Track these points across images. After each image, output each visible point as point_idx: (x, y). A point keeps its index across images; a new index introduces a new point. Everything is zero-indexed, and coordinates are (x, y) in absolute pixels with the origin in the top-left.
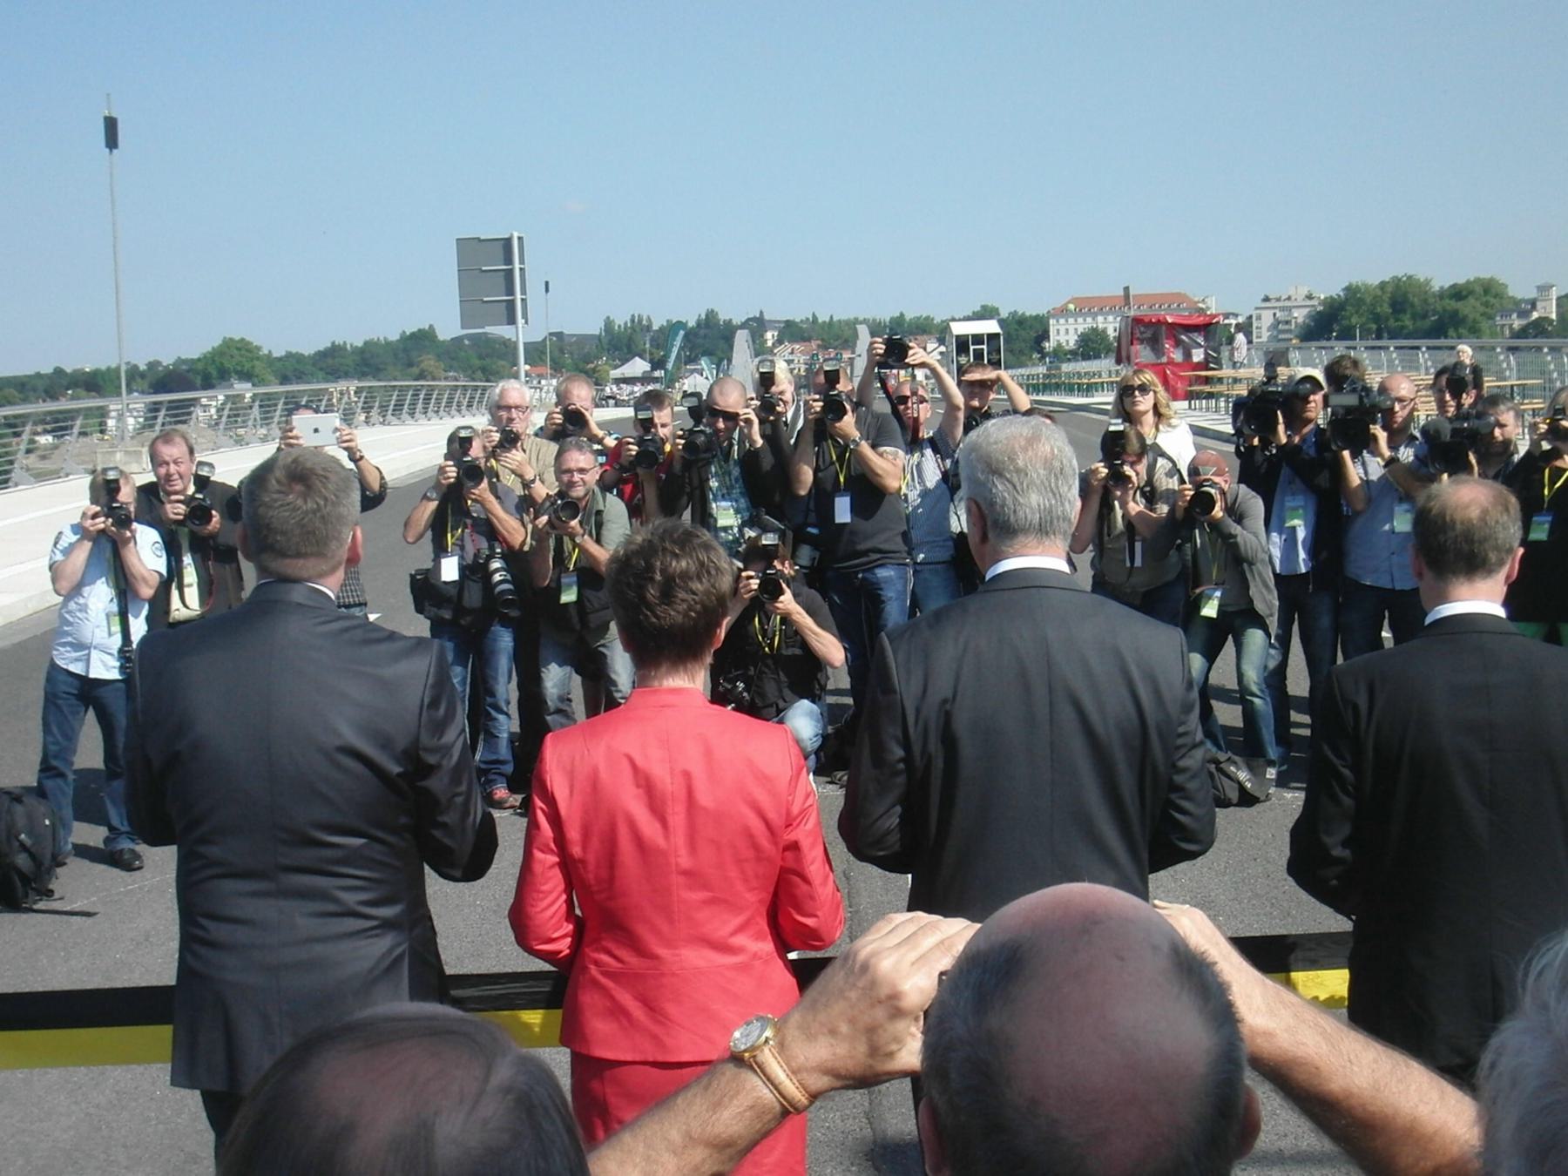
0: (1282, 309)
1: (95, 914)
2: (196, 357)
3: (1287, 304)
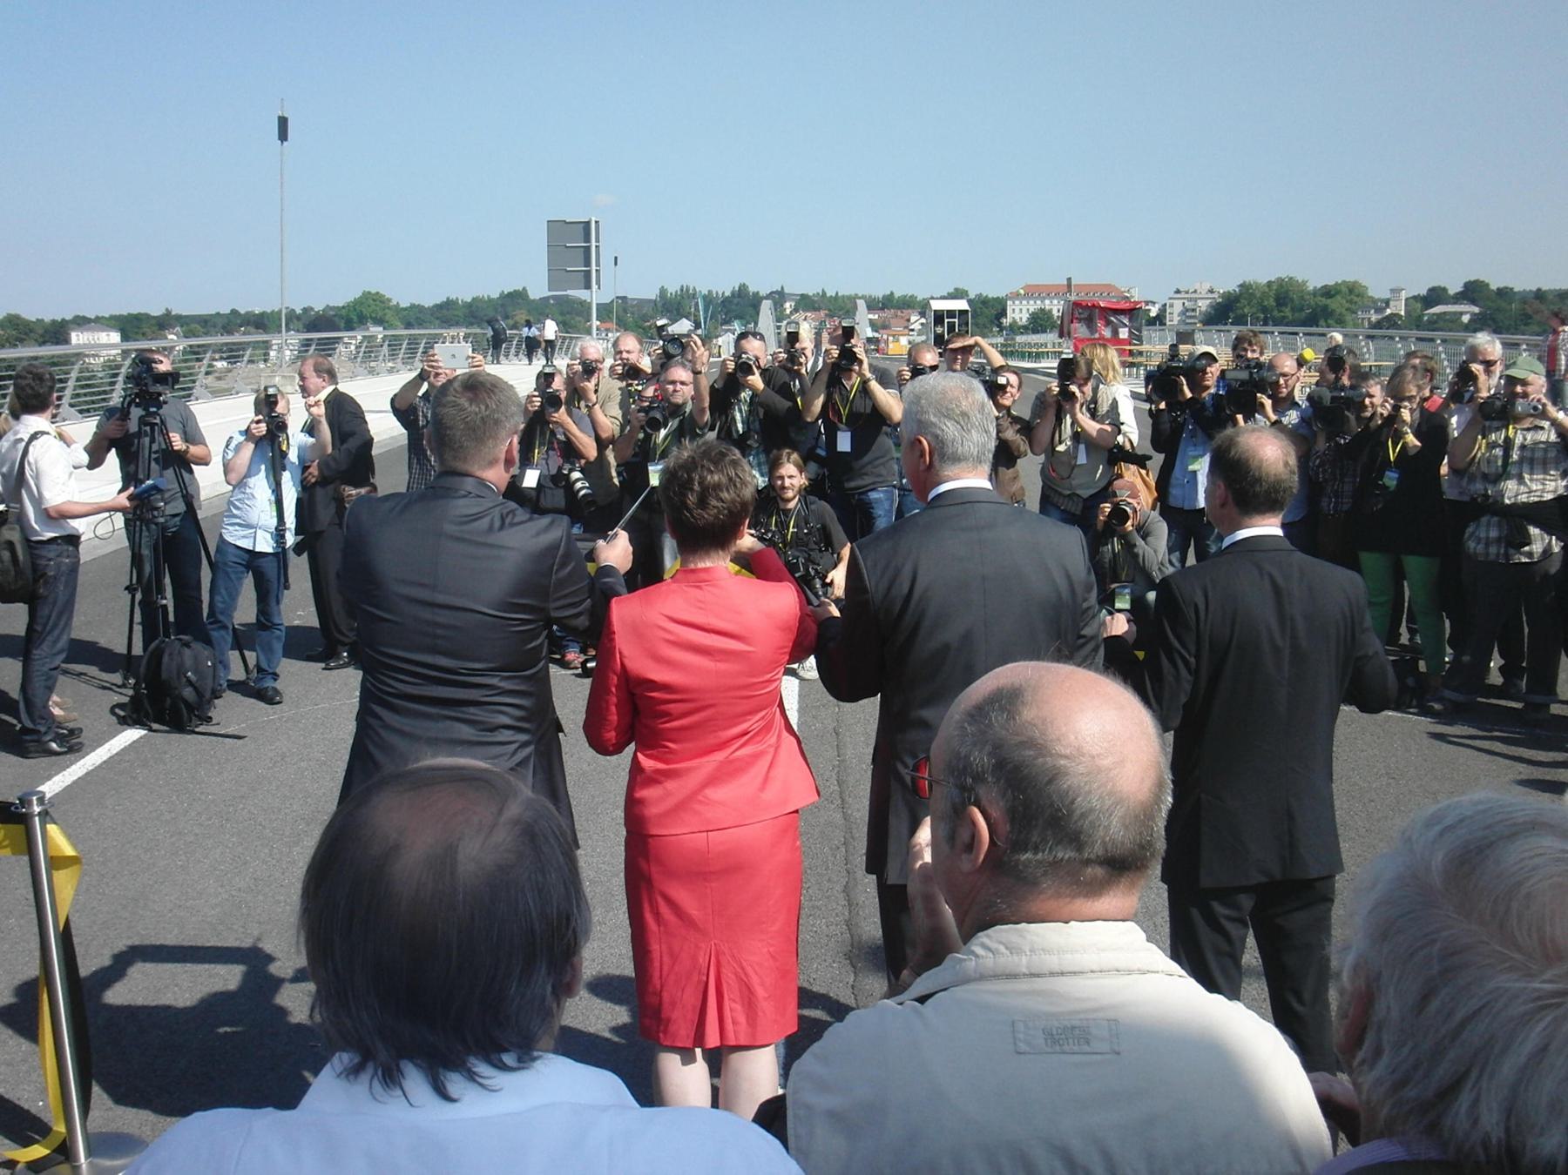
0: (1190, 300)
1: (245, 737)
2: (341, 305)
3: (1194, 296)
